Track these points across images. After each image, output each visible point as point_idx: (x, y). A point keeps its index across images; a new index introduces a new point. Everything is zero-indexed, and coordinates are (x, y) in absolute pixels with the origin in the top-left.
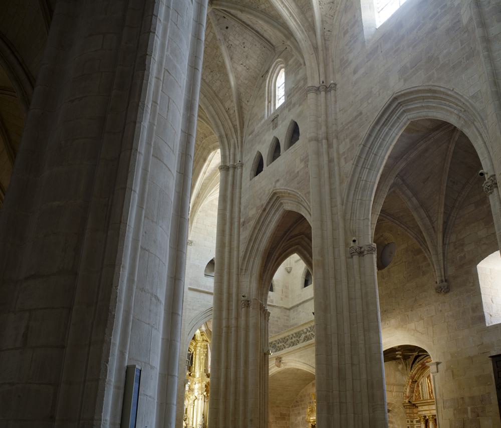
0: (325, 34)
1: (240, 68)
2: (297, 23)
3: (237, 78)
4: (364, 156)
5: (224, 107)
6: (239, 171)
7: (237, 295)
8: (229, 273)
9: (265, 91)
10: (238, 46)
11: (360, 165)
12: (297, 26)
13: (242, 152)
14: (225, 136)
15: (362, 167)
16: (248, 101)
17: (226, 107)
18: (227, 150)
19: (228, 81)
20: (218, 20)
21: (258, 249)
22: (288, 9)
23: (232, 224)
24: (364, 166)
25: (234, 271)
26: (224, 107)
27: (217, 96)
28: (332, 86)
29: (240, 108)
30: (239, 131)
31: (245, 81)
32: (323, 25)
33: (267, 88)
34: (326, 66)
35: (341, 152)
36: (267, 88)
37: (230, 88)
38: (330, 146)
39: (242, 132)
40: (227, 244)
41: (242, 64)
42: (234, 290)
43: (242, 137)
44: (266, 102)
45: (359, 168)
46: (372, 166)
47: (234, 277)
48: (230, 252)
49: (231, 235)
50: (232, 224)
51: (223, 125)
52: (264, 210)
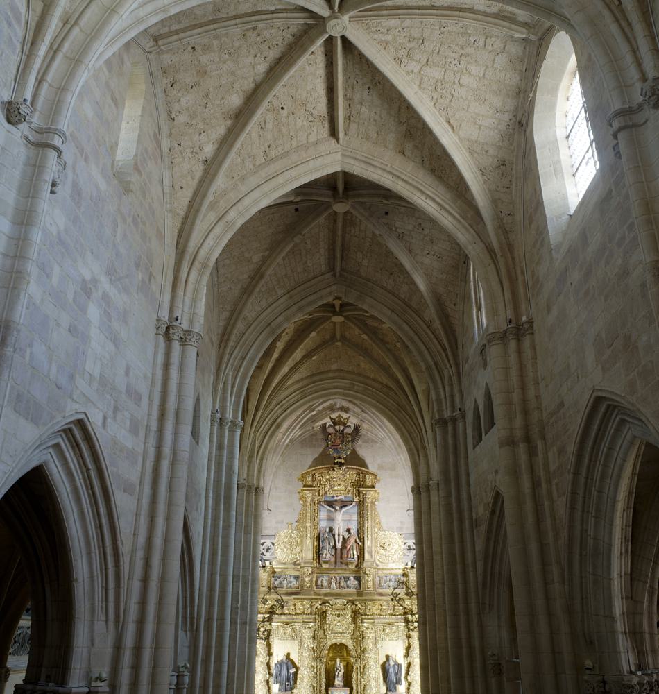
0: (504, 222)
1: (427, 260)
2: (455, 217)
3: (427, 275)
4: (581, 492)
5: (424, 321)
6: (460, 425)
7: (483, 652)
8: (467, 612)
9: (471, 289)
10: (413, 230)
11: (579, 506)
12: (278, 450)
13: (461, 391)
14: (434, 367)
15: (583, 511)
16: (455, 305)
18: (441, 390)
19: (413, 282)
20: (370, 208)
21: (500, 573)
22: (434, 200)
23: (461, 521)
24: (586, 510)
25: (473, 606)
26: (424, 321)
27: (409, 306)
28: (526, 326)
30: (451, 358)
31: (441, 276)
32: (496, 206)
33: (472, 284)
34: (513, 281)
35: (553, 468)
36: (472, 284)
38: (532, 452)
39: (455, 356)
40: (458, 560)
41: (428, 254)
42: (476, 643)
43: (457, 365)
44: (475, 310)
47: (474, 619)
48: (464, 572)
49: (462, 541)
50: (461, 521)
52: (493, 513)
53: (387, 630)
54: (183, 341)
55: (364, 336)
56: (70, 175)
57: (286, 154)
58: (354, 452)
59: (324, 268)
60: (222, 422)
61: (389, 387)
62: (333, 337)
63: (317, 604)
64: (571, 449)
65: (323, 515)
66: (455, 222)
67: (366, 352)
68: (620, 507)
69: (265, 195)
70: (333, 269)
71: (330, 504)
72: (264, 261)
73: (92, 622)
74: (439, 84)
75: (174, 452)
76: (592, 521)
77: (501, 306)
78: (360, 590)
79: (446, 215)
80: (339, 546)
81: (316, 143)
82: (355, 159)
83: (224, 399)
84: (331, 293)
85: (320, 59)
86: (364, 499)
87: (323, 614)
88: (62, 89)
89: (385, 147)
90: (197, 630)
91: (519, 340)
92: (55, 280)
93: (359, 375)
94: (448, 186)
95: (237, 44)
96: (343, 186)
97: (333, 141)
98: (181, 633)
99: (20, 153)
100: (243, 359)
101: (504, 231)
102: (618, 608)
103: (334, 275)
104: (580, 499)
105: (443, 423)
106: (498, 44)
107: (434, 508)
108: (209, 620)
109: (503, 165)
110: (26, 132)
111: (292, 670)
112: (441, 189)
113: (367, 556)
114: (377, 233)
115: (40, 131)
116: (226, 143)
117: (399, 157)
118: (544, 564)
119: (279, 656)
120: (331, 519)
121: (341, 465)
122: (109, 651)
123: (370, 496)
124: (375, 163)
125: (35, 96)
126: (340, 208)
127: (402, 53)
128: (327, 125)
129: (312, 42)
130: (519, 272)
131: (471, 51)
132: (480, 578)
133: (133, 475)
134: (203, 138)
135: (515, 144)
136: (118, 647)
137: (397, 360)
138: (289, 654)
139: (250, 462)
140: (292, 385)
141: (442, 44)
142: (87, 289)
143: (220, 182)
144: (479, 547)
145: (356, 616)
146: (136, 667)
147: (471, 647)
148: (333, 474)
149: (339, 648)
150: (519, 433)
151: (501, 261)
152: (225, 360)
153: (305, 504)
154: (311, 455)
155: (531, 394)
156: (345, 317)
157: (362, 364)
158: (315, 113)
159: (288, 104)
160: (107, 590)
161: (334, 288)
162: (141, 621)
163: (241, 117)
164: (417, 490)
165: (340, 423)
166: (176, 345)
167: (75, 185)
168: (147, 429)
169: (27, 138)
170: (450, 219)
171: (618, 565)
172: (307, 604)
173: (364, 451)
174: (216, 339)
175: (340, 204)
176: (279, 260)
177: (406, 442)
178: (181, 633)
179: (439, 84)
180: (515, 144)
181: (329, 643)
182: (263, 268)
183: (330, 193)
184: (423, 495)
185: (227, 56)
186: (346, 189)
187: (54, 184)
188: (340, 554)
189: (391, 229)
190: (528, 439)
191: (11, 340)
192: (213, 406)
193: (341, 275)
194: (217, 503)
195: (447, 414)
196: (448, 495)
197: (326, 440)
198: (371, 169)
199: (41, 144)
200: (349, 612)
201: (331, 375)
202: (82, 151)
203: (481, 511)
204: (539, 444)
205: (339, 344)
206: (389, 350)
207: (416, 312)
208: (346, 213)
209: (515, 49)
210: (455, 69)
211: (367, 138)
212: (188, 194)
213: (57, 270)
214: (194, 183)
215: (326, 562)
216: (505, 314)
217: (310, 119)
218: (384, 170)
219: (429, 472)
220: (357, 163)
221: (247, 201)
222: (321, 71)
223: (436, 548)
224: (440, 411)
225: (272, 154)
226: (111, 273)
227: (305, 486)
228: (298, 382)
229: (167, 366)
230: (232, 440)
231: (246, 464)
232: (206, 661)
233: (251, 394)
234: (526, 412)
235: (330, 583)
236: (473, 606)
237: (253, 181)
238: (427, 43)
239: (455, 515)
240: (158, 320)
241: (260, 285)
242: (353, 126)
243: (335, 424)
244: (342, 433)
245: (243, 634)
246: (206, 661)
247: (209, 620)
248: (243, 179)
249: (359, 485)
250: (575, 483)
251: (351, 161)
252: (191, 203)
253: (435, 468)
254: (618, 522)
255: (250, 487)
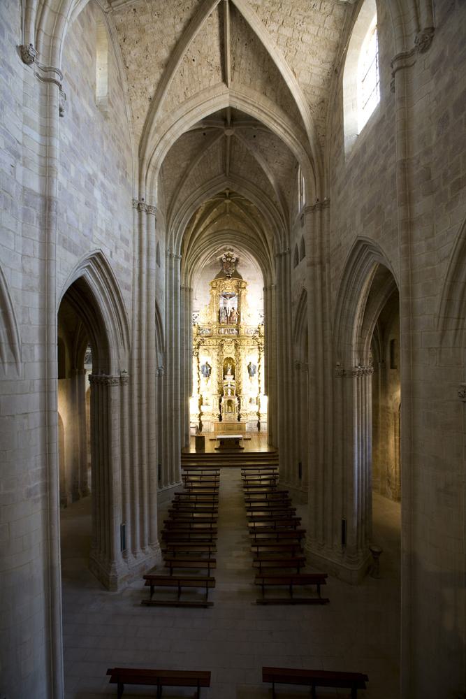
1: (276, 166)
3: (276, 175)
4: (344, 288)
5: (272, 201)
6: (288, 256)
7: (292, 360)
11: (343, 295)
13: (289, 240)
17: (274, 200)
22: (281, 126)
23: (286, 303)
25: (289, 341)
26: (272, 201)
27: (265, 193)
28: (326, 203)
29: (283, 200)
30: (285, 221)
34: (321, 177)
35: (332, 277)
37: (271, 185)
38: (323, 269)
39: (288, 221)
42: (290, 357)
43: (288, 227)
45: (342, 298)
46: (352, 297)
47: (290, 346)
49: (286, 312)
50: (286, 303)
51: (274, 217)
52: (301, 299)
53: (251, 352)
54: (148, 212)
55: (241, 211)
56: (70, 103)
57: (197, 95)
58: (236, 271)
59: (220, 171)
60: (171, 256)
61: (253, 239)
62: (225, 212)
63: (219, 341)
64: (342, 268)
65: (221, 301)
66: (293, 141)
67: (242, 220)
68: (362, 295)
69: (186, 123)
70: (224, 172)
71: (225, 296)
72: (188, 166)
73: (118, 349)
74: (289, 41)
75: (148, 270)
76: (348, 302)
77: (313, 192)
78: (238, 335)
79: (288, 136)
80: (229, 315)
81: (215, 87)
82: (238, 98)
83: (171, 244)
84: (224, 186)
85: (215, 20)
86: (241, 294)
87: (222, 345)
88: (53, 38)
89: (255, 90)
90: (166, 352)
91: (321, 211)
92: (73, 174)
93: (238, 232)
94: (290, 117)
95: (162, 7)
96: (229, 118)
97: (224, 86)
98: (159, 354)
99: (36, 86)
100: (180, 223)
101: (319, 145)
102: (354, 341)
103: (226, 175)
104: (344, 292)
105: (280, 256)
106: (329, 8)
107: (273, 298)
108: (171, 348)
109: (323, 102)
110: (37, 71)
111: (209, 369)
112: (286, 119)
113: (242, 320)
114: (249, 149)
115: (45, 70)
116: (162, 85)
117: (263, 97)
118: (323, 321)
119: (202, 363)
120: (225, 303)
121: (229, 277)
122: (127, 361)
123: (243, 292)
124: (249, 101)
125: (37, 42)
126: (229, 133)
127: (267, 16)
128: (220, 74)
129: (211, 6)
130: (325, 170)
131: (311, 13)
132: (293, 329)
133: (130, 282)
134: (147, 82)
135: (331, 87)
136: (131, 359)
137: (258, 223)
138: (207, 363)
139: (186, 276)
140: (205, 237)
141: (293, 7)
142: (91, 179)
143: (160, 114)
144: (294, 314)
145: (237, 346)
146: (140, 367)
147: (287, 358)
148: (226, 282)
149: (229, 359)
150: (317, 260)
151: (316, 165)
152: (171, 223)
153: (213, 297)
154: (215, 273)
155: (325, 239)
156: (232, 200)
157: (240, 226)
158: (213, 63)
159: (197, 58)
160: (123, 334)
161: (226, 183)
162: (140, 348)
163: (169, 66)
164: (265, 289)
165: (229, 257)
166: (144, 214)
167: (74, 112)
168: (134, 258)
169: (38, 75)
170: (290, 138)
171: (357, 322)
172: (214, 341)
173: (241, 271)
174: (165, 212)
175: (230, 130)
176: (196, 166)
177: (261, 266)
178: (159, 354)
179: (289, 41)
180: (331, 87)
181: (225, 357)
182: (188, 171)
183: (223, 123)
184: (269, 291)
185: (156, 17)
186: (232, 120)
187: (61, 110)
188: (229, 319)
189: (256, 146)
190: (321, 263)
191: (54, 207)
192: (166, 248)
193: (229, 176)
194: (171, 298)
195: (282, 251)
196: (280, 291)
197: (223, 265)
198: (246, 105)
199: (48, 79)
200: (233, 344)
201: (224, 232)
202: (74, 88)
203: (296, 298)
204: (327, 265)
205: (228, 215)
206: (254, 218)
207: (268, 196)
208: (232, 136)
209: (338, 11)
210: (300, 29)
211: (244, 83)
212: (141, 122)
213: (72, 166)
214: (145, 114)
215: (223, 323)
216: (316, 195)
217: (211, 68)
218: (254, 106)
219: (271, 281)
220: (238, 101)
221: (176, 127)
222: (216, 31)
223: (273, 316)
224: (279, 249)
225: (189, 95)
226: (104, 171)
227: (213, 288)
228: (207, 236)
229: (140, 225)
230: (176, 265)
231: (184, 278)
232: (171, 364)
233: (185, 242)
234: (321, 249)
235: (225, 332)
236: (289, 341)
237: (179, 113)
238: (283, 8)
239: (283, 300)
240: (133, 200)
241: (186, 182)
242: (236, 74)
243: (227, 257)
244: (230, 262)
245: (186, 353)
246: (171, 364)
247: (171, 348)
248: (173, 112)
249: (238, 287)
250: (342, 284)
251: (235, 100)
252: (145, 127)
253: (275, 279)
254: (360, 302)
255: (186, 288)
